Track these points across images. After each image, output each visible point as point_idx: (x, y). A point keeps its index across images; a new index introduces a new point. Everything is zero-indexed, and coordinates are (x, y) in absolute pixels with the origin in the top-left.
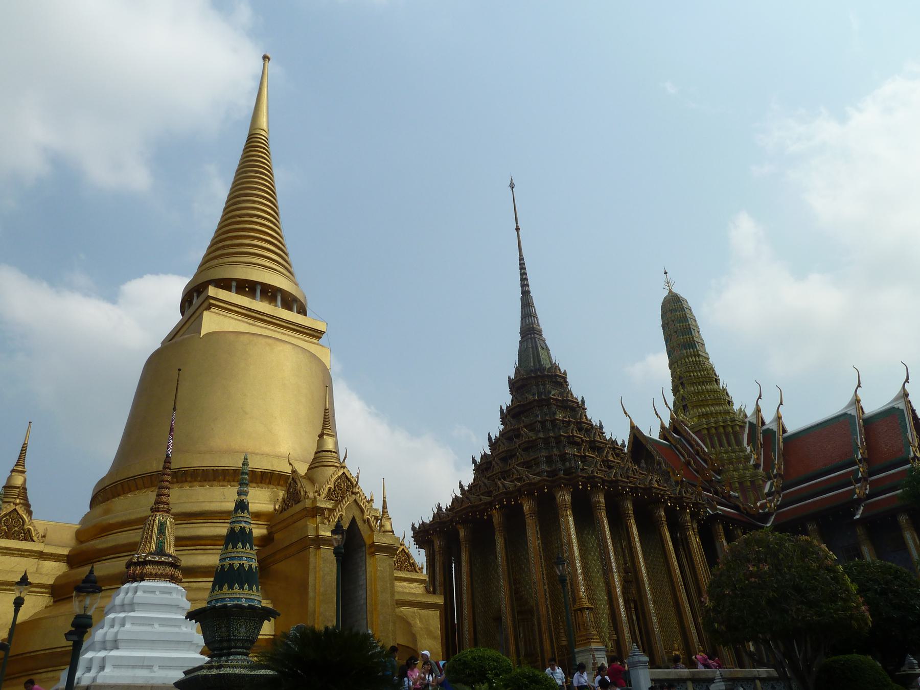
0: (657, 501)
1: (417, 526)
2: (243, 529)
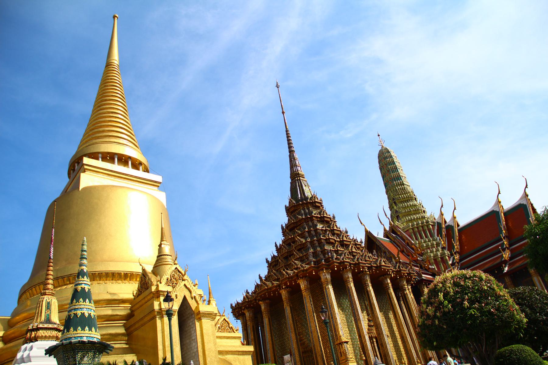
0: (385, 274)
1: (234, 305)
2: (83, 289)
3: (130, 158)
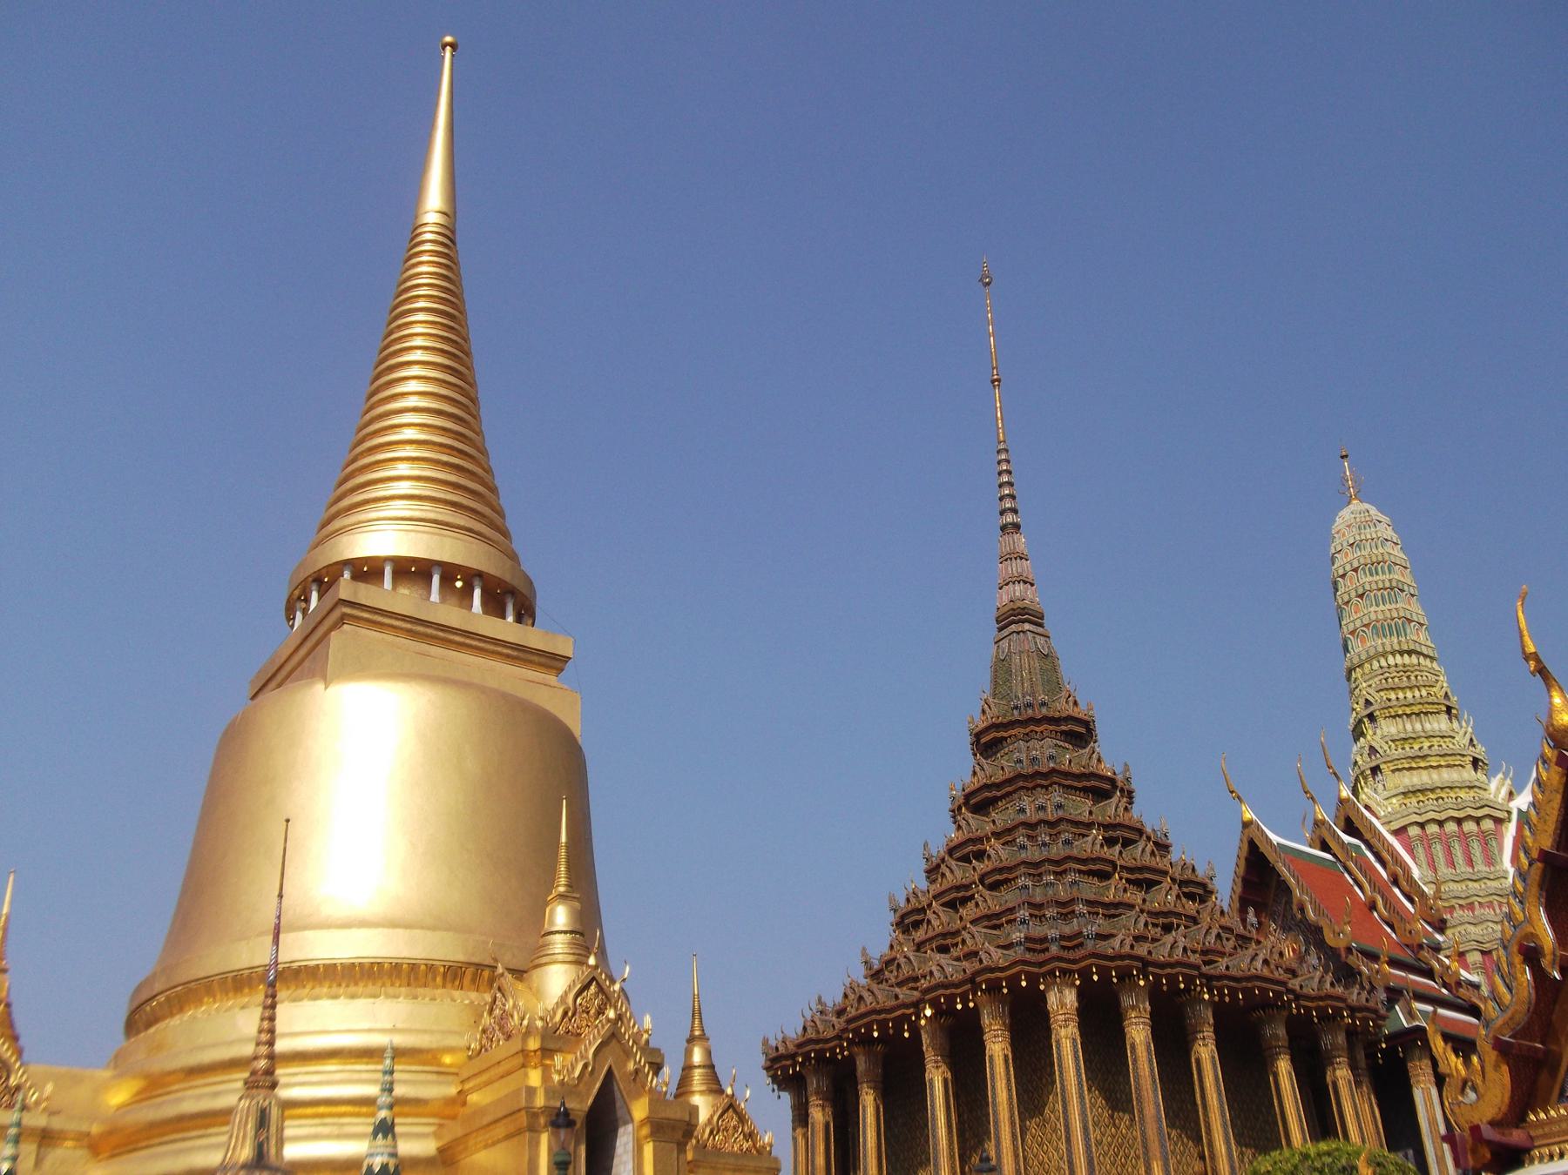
3: (480, 574)
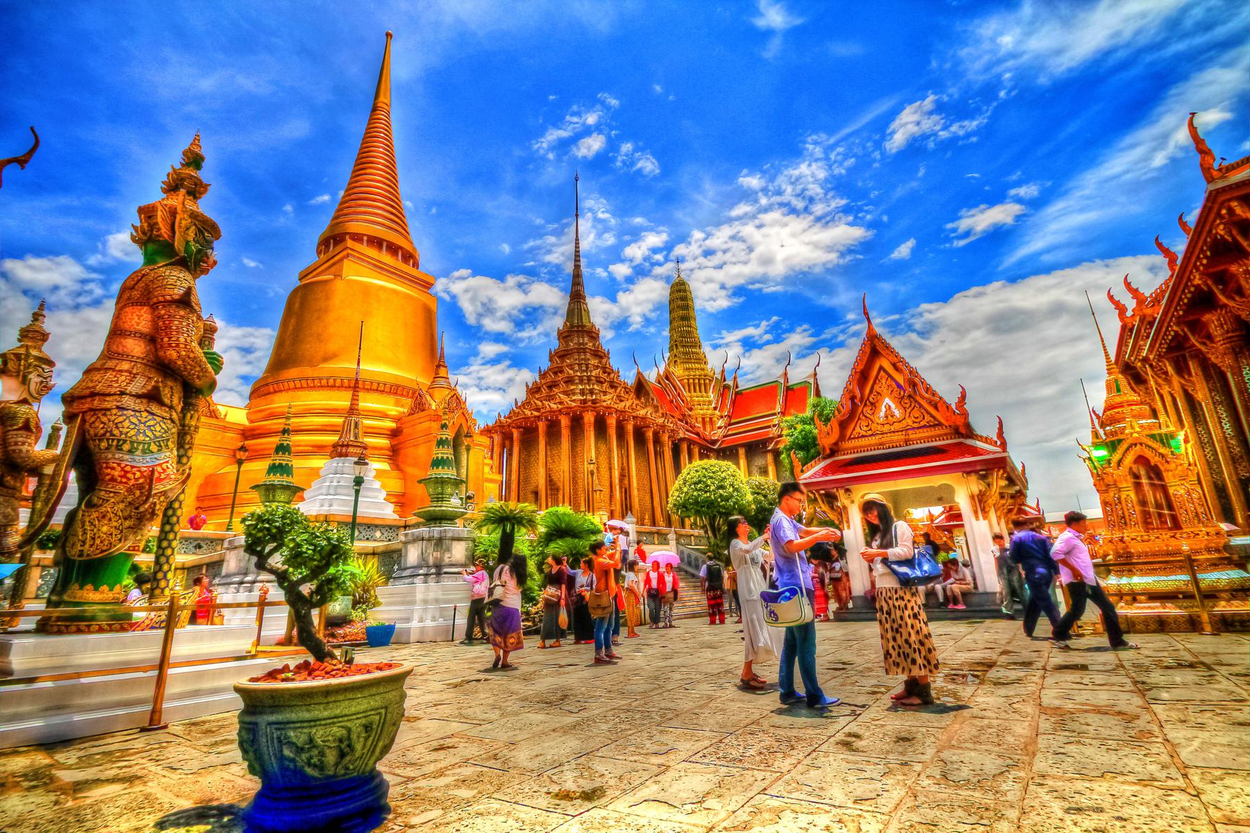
3: (401, 248)
